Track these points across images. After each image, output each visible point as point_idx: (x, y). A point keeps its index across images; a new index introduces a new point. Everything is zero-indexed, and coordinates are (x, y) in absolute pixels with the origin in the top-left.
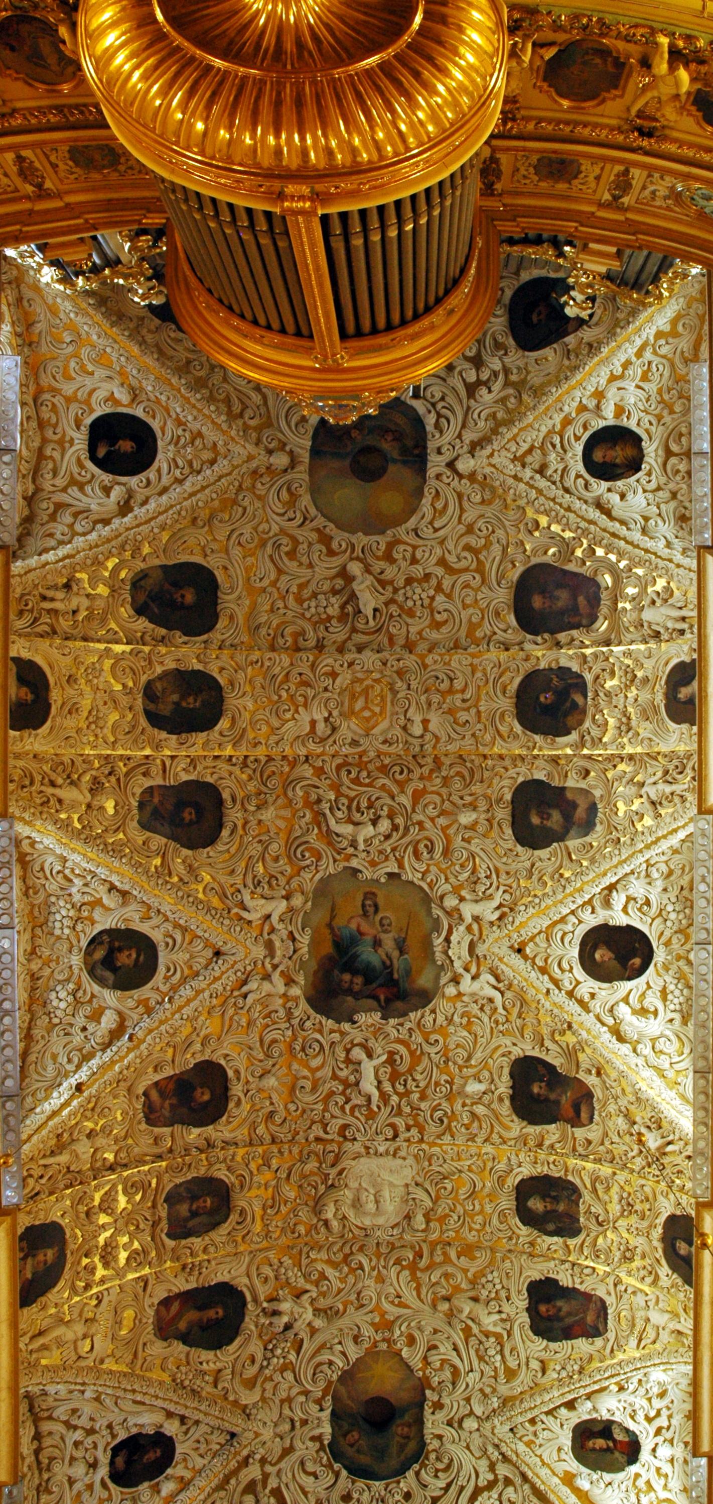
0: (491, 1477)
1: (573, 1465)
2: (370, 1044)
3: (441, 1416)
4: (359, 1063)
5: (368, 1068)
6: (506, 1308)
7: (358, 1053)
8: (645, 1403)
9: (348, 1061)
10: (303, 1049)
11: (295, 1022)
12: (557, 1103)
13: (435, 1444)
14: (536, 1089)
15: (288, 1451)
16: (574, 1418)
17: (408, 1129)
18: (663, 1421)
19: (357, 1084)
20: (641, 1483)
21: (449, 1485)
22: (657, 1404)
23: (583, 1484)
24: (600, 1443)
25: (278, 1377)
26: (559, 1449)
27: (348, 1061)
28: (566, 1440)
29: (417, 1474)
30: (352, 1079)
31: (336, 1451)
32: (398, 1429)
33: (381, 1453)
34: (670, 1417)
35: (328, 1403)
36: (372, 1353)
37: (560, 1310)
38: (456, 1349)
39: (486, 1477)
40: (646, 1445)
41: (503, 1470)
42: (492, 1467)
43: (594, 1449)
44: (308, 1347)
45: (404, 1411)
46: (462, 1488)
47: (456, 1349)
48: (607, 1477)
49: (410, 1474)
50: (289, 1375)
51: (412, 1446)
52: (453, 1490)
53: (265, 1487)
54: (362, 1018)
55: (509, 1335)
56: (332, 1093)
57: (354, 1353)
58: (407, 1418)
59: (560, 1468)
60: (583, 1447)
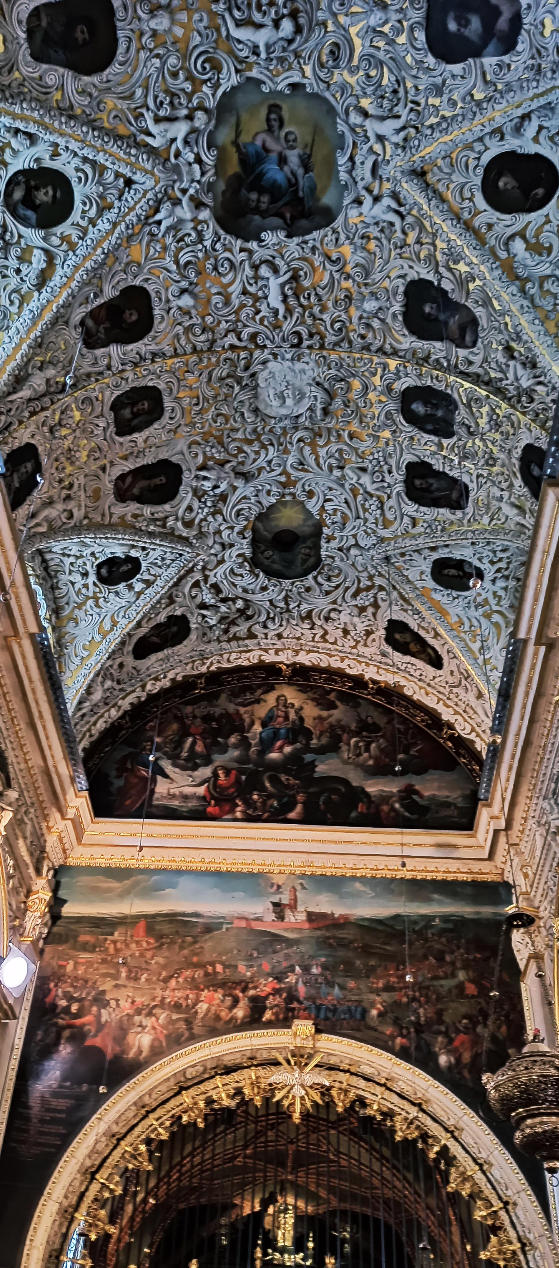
0: (369, 583)
1: (431, 584)
2: (278, 261)
3: (334, 544)
4: (268, 279)
5: (274, 284)
6: (388, 478)
7: (264, 271)
8: (491, 554)
9: (257, 277)
10: (215, 268)
11: (208, 243)
12: (446, 323)
13: (329, 561)
14: (427, 309)
15: (221, 562)
16: (436, 556)
17: (311, 336)
18: (503, 565)
19: (266, 297)
21: (337, 587)
22: (500, 555)
23: (437, 596)
24: (453, 572)
25: (210, 518)
26: (422, 573)
27: (257, 277)
28: (427, 567)
29: (315, 578)
30: (260, 294)
31: (255, 563)
32: (302, 550)
33: (290, 564)
34: (509, 563)
35: (249, 534)
36: (281, 503)
37: (431, 485)
38: (346, 502)
39: (365, 583)
41: (378, 581)
42: (371, 578)
43: (448, 575)
44: (232, 500)
45: (305, 539)
46: (347, 588)
47: (346, 502)
48: (455, 593)
49: (310, 577)
50: (219, 518)
51: (312, 561)
52: (341, 590)
53: (206, 583)
54: (269, 237)
55: (389, 497)
56: (242, 306)
57: (268, 501)
58: (309, 543)
60: (440, 573)
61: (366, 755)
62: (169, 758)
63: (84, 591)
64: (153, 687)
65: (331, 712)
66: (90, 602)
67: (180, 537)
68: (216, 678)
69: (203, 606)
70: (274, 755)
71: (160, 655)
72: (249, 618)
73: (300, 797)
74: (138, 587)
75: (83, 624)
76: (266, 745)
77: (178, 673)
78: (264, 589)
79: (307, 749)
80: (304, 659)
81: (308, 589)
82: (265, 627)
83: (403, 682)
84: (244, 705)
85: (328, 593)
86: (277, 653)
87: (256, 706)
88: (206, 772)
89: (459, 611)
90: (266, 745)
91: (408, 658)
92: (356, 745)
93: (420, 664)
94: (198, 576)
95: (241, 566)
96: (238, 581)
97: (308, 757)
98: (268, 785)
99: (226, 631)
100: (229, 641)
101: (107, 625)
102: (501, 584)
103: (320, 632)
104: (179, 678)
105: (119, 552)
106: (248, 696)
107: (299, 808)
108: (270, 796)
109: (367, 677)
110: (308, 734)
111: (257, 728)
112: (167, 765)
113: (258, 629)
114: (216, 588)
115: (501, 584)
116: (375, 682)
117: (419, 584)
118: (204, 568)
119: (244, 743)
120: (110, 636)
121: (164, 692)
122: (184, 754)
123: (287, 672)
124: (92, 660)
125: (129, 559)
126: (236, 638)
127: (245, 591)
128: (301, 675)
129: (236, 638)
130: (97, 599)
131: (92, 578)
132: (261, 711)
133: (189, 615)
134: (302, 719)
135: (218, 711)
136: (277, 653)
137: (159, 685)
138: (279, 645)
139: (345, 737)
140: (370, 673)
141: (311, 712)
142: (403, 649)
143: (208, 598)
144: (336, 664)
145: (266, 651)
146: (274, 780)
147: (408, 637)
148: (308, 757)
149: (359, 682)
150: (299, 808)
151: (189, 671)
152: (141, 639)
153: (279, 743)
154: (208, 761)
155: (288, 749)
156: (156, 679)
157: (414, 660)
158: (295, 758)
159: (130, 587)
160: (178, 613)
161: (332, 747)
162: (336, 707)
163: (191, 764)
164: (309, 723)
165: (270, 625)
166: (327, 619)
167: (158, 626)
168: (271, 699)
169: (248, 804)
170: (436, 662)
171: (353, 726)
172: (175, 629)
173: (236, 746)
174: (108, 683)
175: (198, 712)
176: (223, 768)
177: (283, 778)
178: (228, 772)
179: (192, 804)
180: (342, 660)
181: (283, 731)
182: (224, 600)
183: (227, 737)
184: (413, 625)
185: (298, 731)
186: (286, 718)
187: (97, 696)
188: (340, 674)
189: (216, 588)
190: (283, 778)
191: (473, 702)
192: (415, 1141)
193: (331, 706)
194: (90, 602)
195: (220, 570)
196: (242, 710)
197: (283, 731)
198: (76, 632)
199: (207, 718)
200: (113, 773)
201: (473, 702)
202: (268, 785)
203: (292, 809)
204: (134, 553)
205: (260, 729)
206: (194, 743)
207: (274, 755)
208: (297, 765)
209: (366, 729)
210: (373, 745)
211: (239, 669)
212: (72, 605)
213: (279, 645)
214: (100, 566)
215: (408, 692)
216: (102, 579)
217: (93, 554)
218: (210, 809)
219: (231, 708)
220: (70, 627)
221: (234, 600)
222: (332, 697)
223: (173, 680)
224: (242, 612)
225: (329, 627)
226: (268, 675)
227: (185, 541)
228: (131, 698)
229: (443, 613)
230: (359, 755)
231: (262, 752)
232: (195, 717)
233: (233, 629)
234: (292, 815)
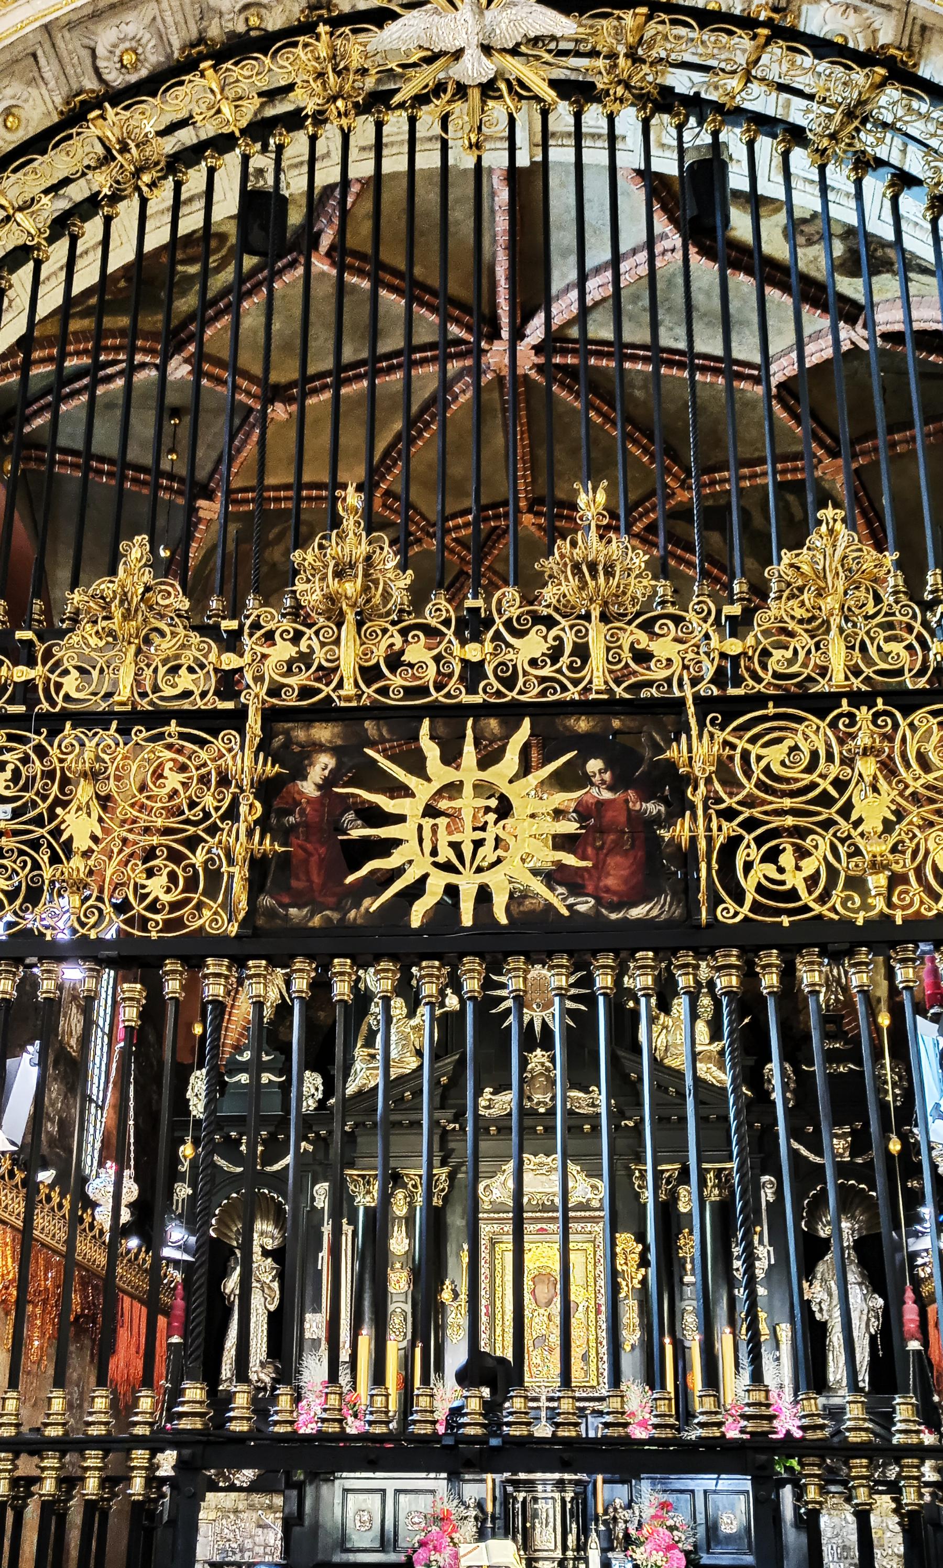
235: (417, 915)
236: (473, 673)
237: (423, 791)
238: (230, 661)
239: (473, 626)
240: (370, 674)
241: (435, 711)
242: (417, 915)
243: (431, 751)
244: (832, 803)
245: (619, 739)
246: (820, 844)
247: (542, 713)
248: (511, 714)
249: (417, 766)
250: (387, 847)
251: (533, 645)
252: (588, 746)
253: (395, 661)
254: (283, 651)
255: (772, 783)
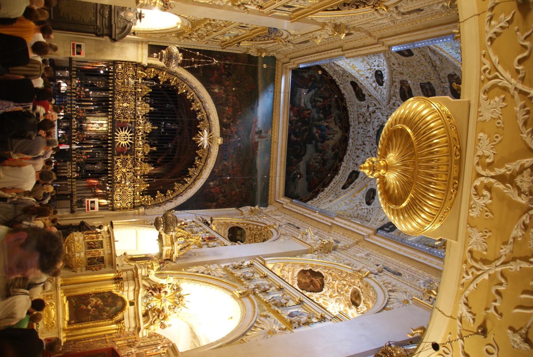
1: (369, 188)
20: (362, 204)
23: (364, 189)
40: (368, 207)
48: (365, 195)
59: (369, 184)
61: (314, 162)
62: (315, 93)
63: (373, 65)
64: (341, 87)
65: (331, 151)
66: (369, 67)
67: (390, 101)
68: (345, 110)
69: (368, 107)
70: (315, 130)
71: (353, 90)
72: (365, 122)
73: (299, 139)
74: (374, 85)
75: (361, 64)
76: (319, 127)
77: (346, 96)
78: (374, 129)
79: (317, 142)
80: (350, 141)
81: (372, 145)
82: (362, 128)
83: (339, 176)
84: (334, 120)
85: (370, 151)
86: (353, 132)
87: (334, 123)
88: (309, 106)
89: (359, 197)
90: (319, 127)
91: (347, 178)
92: (317, 159)
93: (345, 182)
94: (378, 106)
95: (381, 122)
96: (376, 120)
97: (314, 142)
98: (304, 128)
99: (360, 114)
100: (358, 115)
101: (361, 73)
102: (366, 211)
103: (358, 147)
104: (345, 96)
105: (385, 78)
106: (338, 121)
107: (295, 139)
108: (300, 129)
109: (343, 163)
110: (323, 142)
111: (326, 124)
112: (311, 93)
113: (361, 125)
114: (374, 112)
115: (366, 211)
116: (341, 165)
117: (369, 184)
118: (380, 108)
119: (320, 120)
120: (357, 74)
121: (340, 91)
122: (316, 98)
123: (346, 135)
124: (348, 67)
125: (383, 82)
126: (359, 117)
127: (373, 122)
128: (345, 140)
129: (359, 117)
130: (370, 69)
131: (377, 68)
132: (332, 125)
133: (365, 101)
134: (328, 140)
135: (332, 110)
136: (353, 132)
137: (342, 89)
138: (356, 132)
139: (321, 155)
140: (344, 164)
141: (331, 143)
142: (350, 176)
143: (371, 109)
144: (348, 152)
145: (354, 128)
146: (306, 130)
147: (353, 178)
148: (314, 142)
149: (341, 160)
150: (295, 139)
151: (347, 100)
152: (357, 84)
153: (319, 132)
154: (313, 107)
155: (317, 135)
156: (344, 88)
157: (346, 180)
158: (314, 137)
159: (374, 82)
160: (366, 98)
161: (317, 150)
162: (332, 151)
163: (313, 101)
164: (327, 142)
165: (362, 130)
166: (363, 150)
167: (361, 90)
168: (337, 129)
169: (297, 121)
170: (344, 188)
171: (325, 157)
172: (361, 96)
173: (319, 117)
174: (341, 72)
175: (332, 103)
176: (311, 112)
177: (306, 133)
178: (309, 114)
179: (297, 102)
180: (349, 155)
181: (324, 133)
182: (370, 114)
183: (322, 113)
184: (357, 181)
185: (324, 138)
186: (329, 134)
187: (337, 68)
188: (344, 154)
189: (374, 112)
190: (306, 133)
191: (330, 199)
192: (188, 174)
193: (333, 150)
194: (369, 67)
195: (380, 114)
196: (333, 119)
197: (324, 133)
198: (359, 61)
199: (330, 106)
200: (310, 73)
201: (330, 199)
202: (304, 128)
203: (295, 136)
204: (384, 84)
205: (325, 125)
206: (321, 102)
207: (315, 130)
208: (311, 138)
209: (324, 162)
210: (318, 164)
211: (348, 118)
212: (368, 60)
213: (356, 132)
214: (381, 71)
215: (336, 176)
216: (377, 72)
217: (384, 70)
218: (295, 108)
219: (333, 115)
220: (360, 59)
221: (370, 118)
222: (337, 150)
223: (344, 94)
224: (366, 120)
225: (360, 151)
226: (346, 128)
227: (389, 103)
228: (337, 80)
229: (359, 191)
230: (314, 159)
231: (316, 126)
232: (331, 102)
233: (361, 117)
234: (292, 136)
235: (116, 133)
236: (138, 138)
237: (127, 134)
238: (140, 117)
239: (143, 138)
240: (139, 129)
241: (135, 135)
242: (116, 133)
243: (131, 134)
244: (124, 167)
245: (130, 150)
246: (121, 166)
247: (134, 144)
248: (134, 141)
249: (130, 133)
250: (122, 131)
251: (141, 143)
252: (131, 148)
253: (140, 131)
254: (141, 122)
255: (127, 163)
